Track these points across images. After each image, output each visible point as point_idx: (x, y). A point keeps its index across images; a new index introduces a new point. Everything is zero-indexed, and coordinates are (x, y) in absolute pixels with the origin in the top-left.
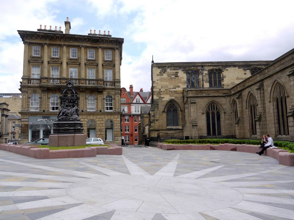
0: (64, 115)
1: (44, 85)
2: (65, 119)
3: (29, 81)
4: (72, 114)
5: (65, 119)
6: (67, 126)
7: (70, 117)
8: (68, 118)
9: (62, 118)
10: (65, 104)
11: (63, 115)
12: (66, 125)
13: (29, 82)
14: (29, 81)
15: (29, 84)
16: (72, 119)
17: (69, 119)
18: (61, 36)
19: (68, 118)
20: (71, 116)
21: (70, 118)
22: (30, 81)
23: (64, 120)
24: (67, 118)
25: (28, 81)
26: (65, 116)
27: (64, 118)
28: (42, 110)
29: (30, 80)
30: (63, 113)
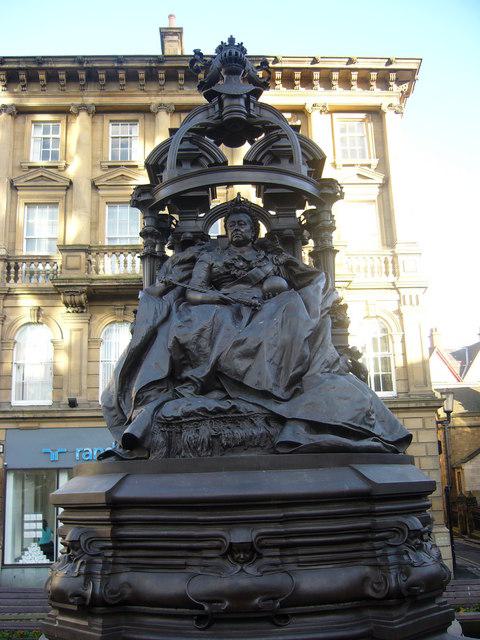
0: (200, 372)
1: (71, 280)
2: (206, 431)
3: (13, 270)
4: (305, 364)
5: (206, 431)
6: (250, 553)
7: (280, 409)
8: (249, 418)
9: (168, 423)
10: (193, 261)
11: (174, 378)
12: (241, 536)
13: (9, 273)
14: (13, 270)
15: (12, 280)
16: (316, 427)
17: (260, 429)
18: (148, 65)
19: (249, 418)
20: (296, 384)
21: (282, 421)
22: (17, 268)
23: (193, 447)
24: (234, 417)
25: (9, 268)
26: (204, 389)
27: (205, 415)
28: (66, 400)
29: (12, 264)
30: (182, 356)
